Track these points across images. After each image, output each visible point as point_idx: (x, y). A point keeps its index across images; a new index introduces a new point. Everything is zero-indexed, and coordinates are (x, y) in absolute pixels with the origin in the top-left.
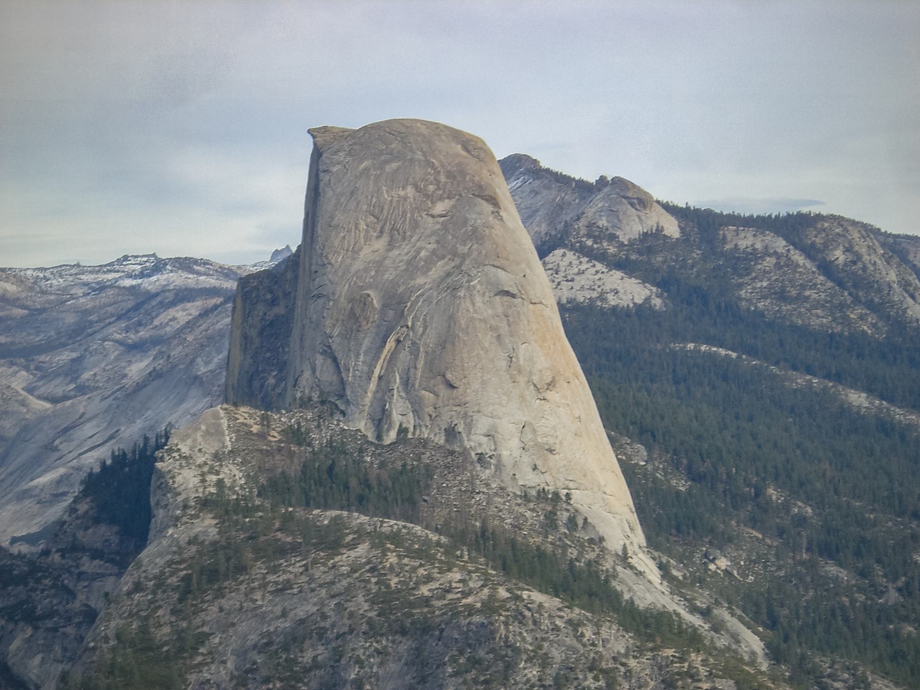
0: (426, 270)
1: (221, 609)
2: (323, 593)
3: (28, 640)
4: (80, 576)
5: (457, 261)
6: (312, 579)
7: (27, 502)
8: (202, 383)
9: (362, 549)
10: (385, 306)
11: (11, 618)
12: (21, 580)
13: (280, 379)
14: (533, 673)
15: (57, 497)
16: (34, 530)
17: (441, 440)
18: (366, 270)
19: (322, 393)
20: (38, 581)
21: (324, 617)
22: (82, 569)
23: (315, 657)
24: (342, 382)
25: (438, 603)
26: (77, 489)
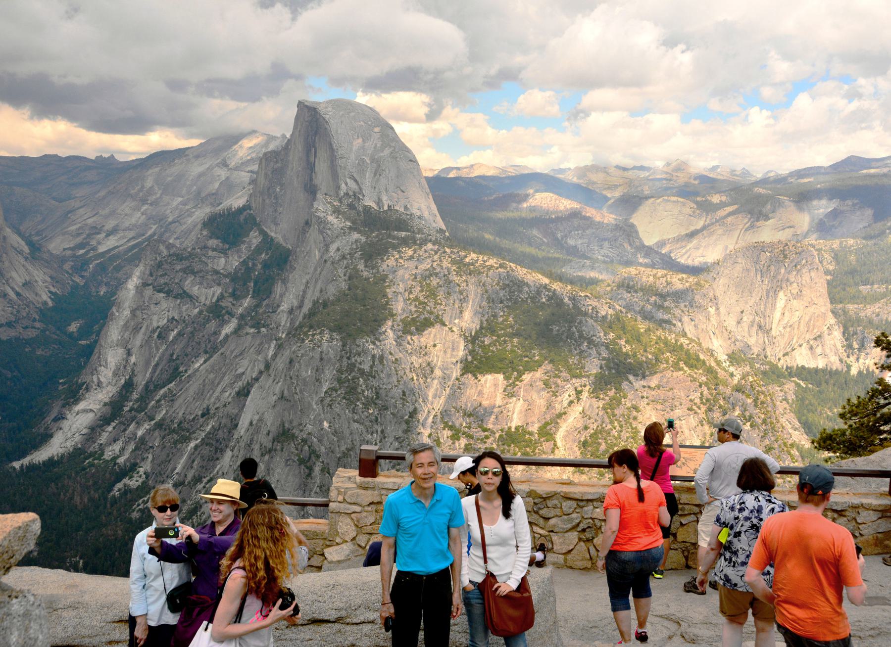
0: (382, 151)
1: (388, 266)
2: (429, 260)
3: (192, 281)
4: (209, 257)
5: (393, 149)
6: (419, 255)
7: (67, 236)
8: (132, 197)
9: (430, 246)
10: (371, 162)
11: (185, 272)
12: (187, 258)
13: (281, 190)
14: (527, 289)
15: (79, 235)
16: (72, 246)
17: (402, 210)
18: (358, 149)
19: (354, 192)
20: (193, 259)
21: (434, 269)
22: (210, 255)
23: (438, 283)
24: (360, 188)
25: (477, 265)
26: (199, 226)
